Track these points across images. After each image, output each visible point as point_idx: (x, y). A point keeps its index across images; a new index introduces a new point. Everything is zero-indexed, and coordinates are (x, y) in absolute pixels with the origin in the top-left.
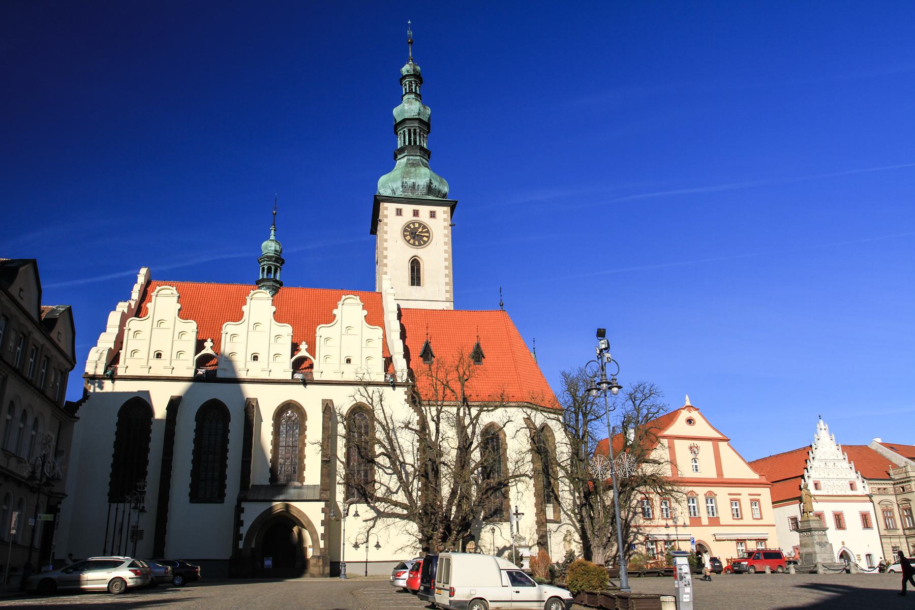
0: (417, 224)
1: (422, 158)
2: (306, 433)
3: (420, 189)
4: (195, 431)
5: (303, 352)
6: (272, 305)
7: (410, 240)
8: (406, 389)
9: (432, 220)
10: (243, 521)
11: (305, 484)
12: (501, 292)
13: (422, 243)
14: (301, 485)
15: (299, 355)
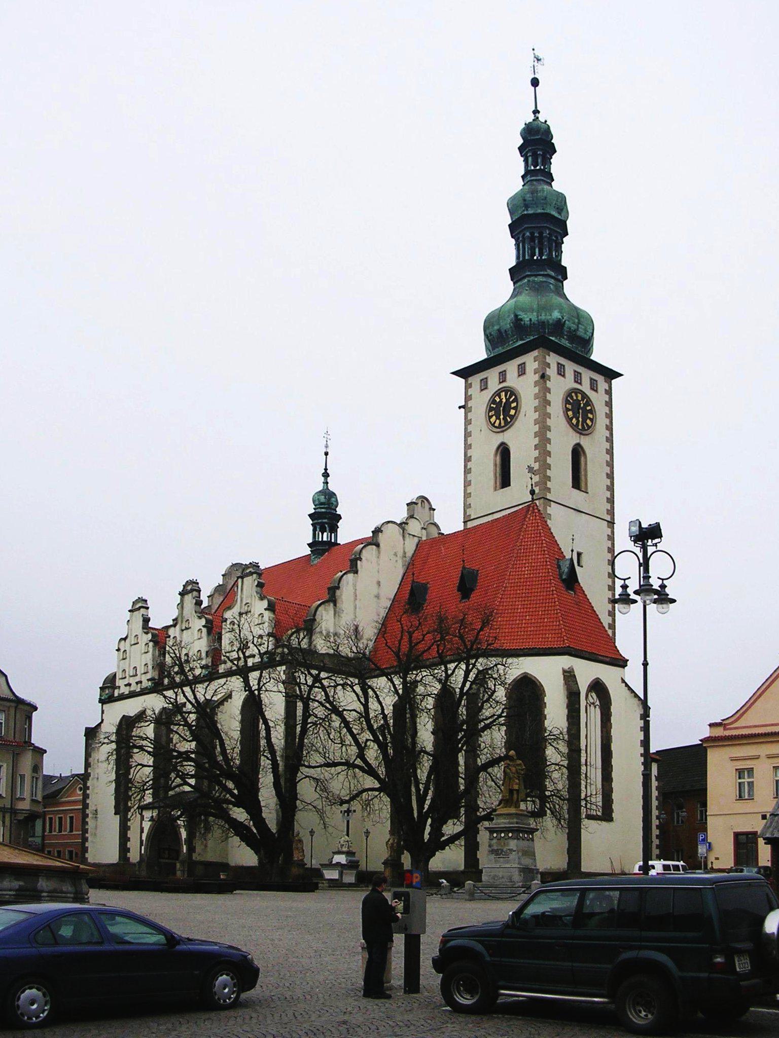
0: (504, 393)
1: (532, 279)
3: (509, 336)
13: (509, 420)
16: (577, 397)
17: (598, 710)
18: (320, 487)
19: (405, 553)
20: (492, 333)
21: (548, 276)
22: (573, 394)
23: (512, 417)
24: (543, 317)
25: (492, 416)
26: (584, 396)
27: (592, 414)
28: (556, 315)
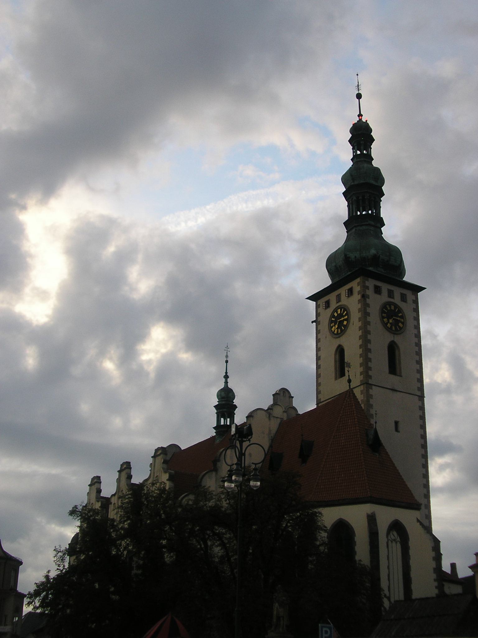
0: (339, 310)
16: (390, 307)
17: (399, 545)
18: (222, 386)
19: (270, 430)
21: (369, 225)
22: (388, 306)
23: (345, 326)
26: (396, 306)
27: (403, 319)
28: (373, 251)
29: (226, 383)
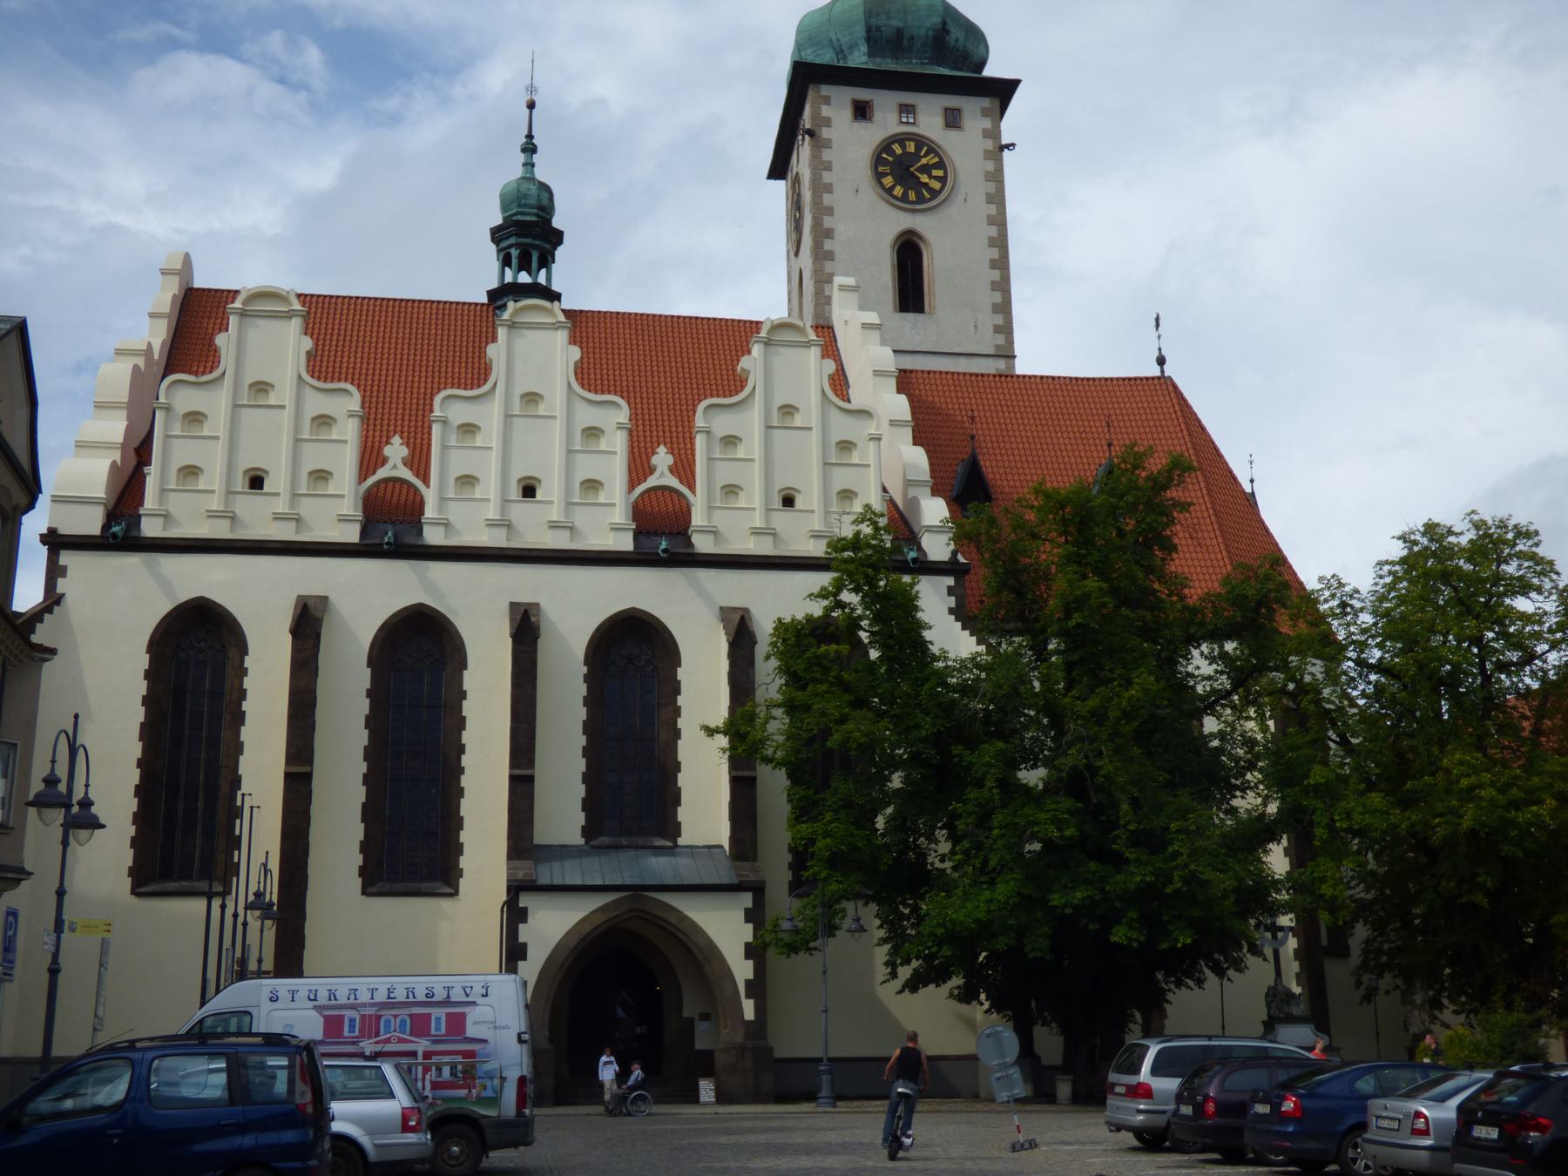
0: (912, 144)
2: (681, 700)
3: (914, 48)
4: (370, 694)
5: (662, 473)
6: (570, 343)
7: (893, 188)
8: (950, 581)
9: (953, 134)
10: (525, 945)
11: (681, 841)
12: (1157, 325)
14: (669, 844)
15: (652, 481)
20: (883, 28)
24: (970, 46)
25: (885, 175)
29: (529, 165)
